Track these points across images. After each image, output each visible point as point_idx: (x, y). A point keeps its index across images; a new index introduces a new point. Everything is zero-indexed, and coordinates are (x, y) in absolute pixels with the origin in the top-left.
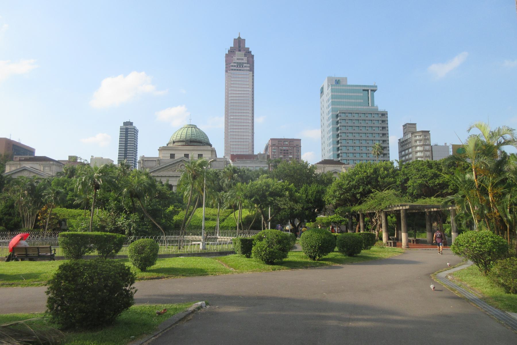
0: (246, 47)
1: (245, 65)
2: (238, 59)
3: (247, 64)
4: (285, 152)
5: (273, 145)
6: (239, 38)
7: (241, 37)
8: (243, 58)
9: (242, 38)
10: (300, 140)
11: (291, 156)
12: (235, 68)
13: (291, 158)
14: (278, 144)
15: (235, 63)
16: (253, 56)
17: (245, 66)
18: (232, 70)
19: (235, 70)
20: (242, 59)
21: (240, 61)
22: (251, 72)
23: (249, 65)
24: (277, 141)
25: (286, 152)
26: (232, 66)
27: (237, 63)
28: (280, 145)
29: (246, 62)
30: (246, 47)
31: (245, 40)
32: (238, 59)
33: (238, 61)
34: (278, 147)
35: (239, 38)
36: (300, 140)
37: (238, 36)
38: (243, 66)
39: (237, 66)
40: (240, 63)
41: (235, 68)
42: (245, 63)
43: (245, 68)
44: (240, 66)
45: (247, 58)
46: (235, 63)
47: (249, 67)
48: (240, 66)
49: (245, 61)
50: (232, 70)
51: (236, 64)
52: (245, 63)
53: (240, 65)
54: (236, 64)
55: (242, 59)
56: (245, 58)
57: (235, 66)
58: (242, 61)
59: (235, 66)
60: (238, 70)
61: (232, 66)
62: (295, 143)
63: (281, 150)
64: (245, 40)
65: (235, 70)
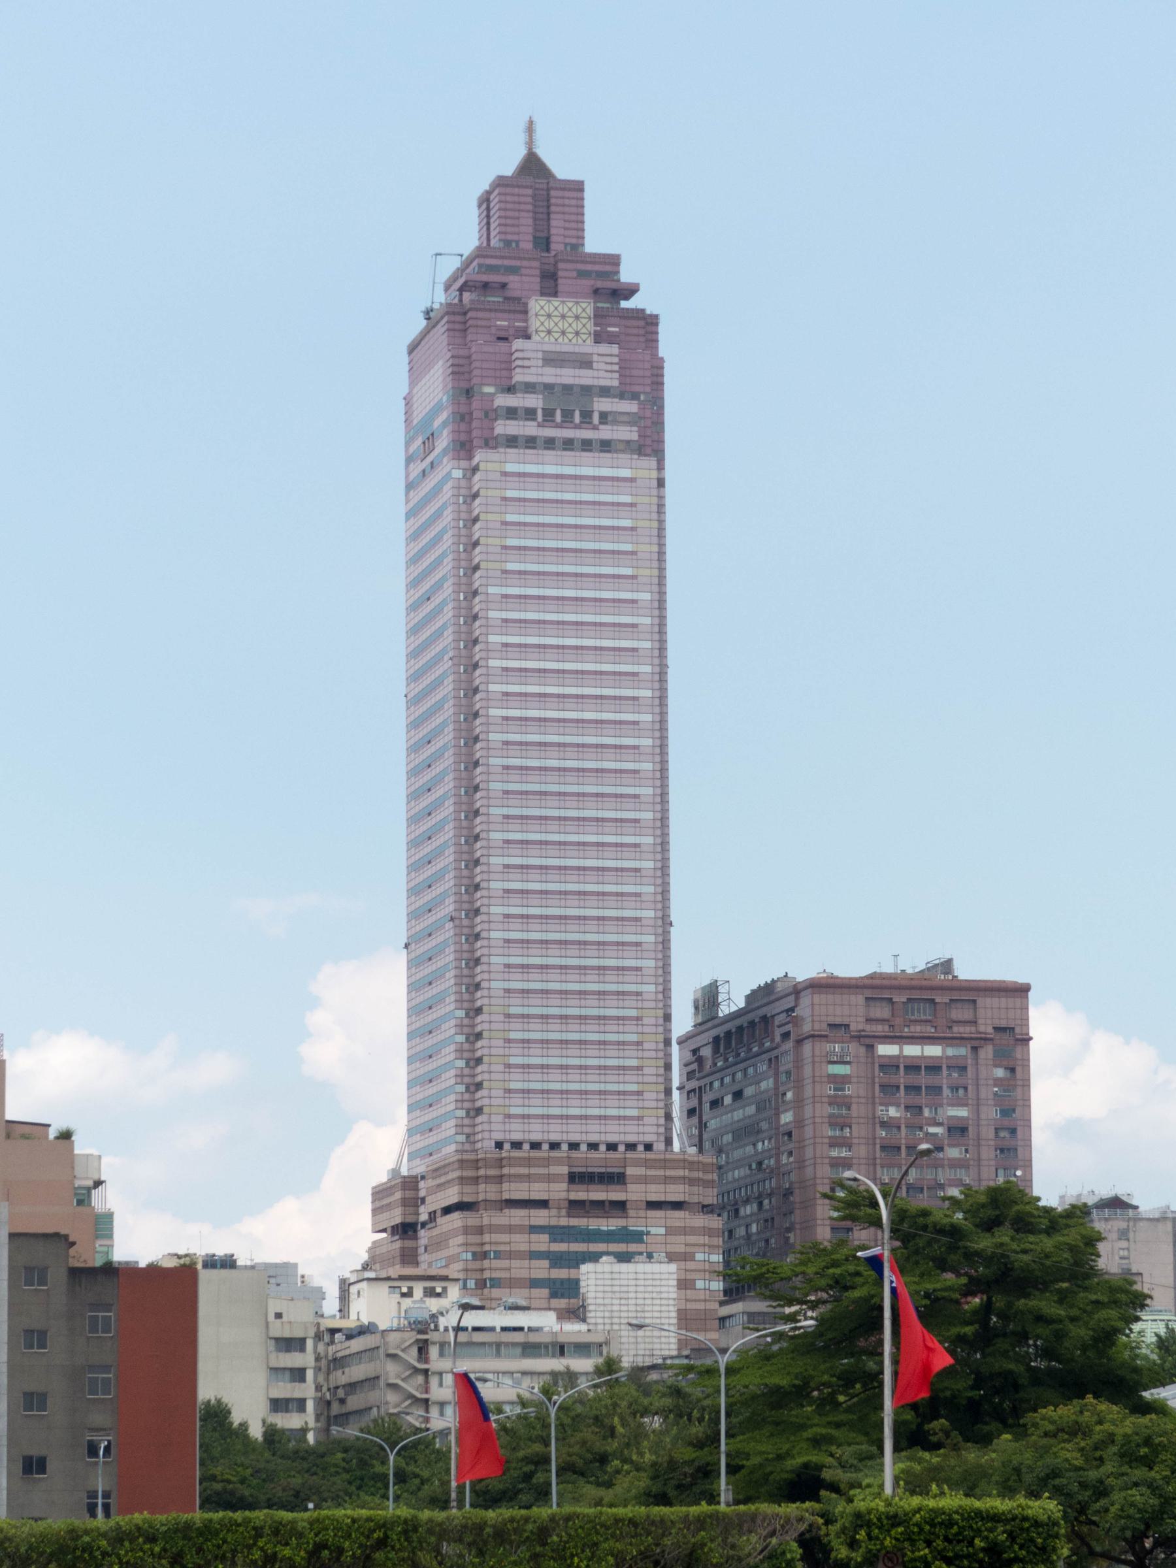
0: (592, 245)
1: (602, 405)
3: (621, 396)
4: (913, 1079)
5: (832, 1026)
6: (532, 165)
7: (543, 153)
8: (586, 346)
9: (562, 170)
10: (1022, 991)
11: (963, 1112)
12: (530, 429)
13: (958, 1130)
14: (869, 1020)
15: (530, 388)
16: (648, 324)
17: (604, 416)
18: (512, 441)
20: (585, 363)
22: (653, 463)
23: (631, 407)
24: (860, 999)
25: (923, 1079)
26: (511, 413)
27: (549, 387)
28: (880, 1029)
29: (613, 381)
30: (592, 245)
31: (577, 187)
32: (552, 360)
33: (550, 375)
34: (871, 1048)
35: (532, 165)
36: (1022, 991)
37: (520, 153)
38: (587, 415)
39: (549, 414)
40: (567, 389)
41: (530, 429)
42: (605, 392)
44: (568, 415)
45: (615, 349)
46: (530, 388)
47: (632, 420)
48: (568, 415)
49: (603, 374)
50: (512, 441)
51: (533, 401)
52: (605, 392)
54: (533, 401)
55: (585, 363)
56: (604, 348)
57: (530, 414)
58: (585, 377)
59: (530, 414)
60: (550, 443)
61: (511, 413)
62: (990, 1013)
63: (890, 1065)
64: (577, 187)
65: (531, 442)
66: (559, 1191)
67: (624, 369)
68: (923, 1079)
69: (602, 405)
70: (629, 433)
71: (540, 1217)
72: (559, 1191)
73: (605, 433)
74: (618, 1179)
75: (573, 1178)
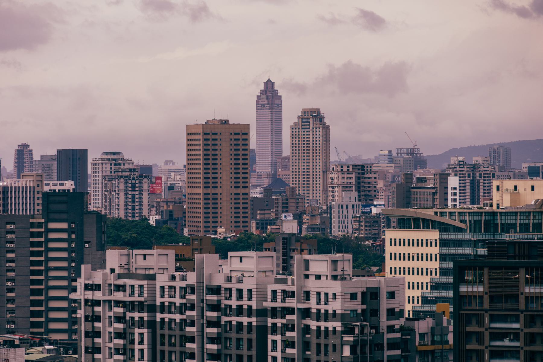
1: (266, 105)
2: (262, 101)
12: (260, 108)
17: (266, 106)
19: (260, 109)
20: (265, 101)
21: (263, 103)
23: (268, 105)
33: (262, 103)
41: (260, 108)
42: (266, 104)
43: (266, 108)
46: (260, 104)
51: (260, 105)
52: (266, 104)
53: (263, 105)
54: (260, 105)
57: (260, 106)
58: (265, 103)
60: (262, 109)
65: (260, 109)
66: (256, 177)
67: (268, 102)
68: (286, 166)
69: (266, 105)
70: (268, 108)
71: (255, 179)
72: (256, 177)
73: (266, 108)
74: (261, 176)
75: (258, 176)
